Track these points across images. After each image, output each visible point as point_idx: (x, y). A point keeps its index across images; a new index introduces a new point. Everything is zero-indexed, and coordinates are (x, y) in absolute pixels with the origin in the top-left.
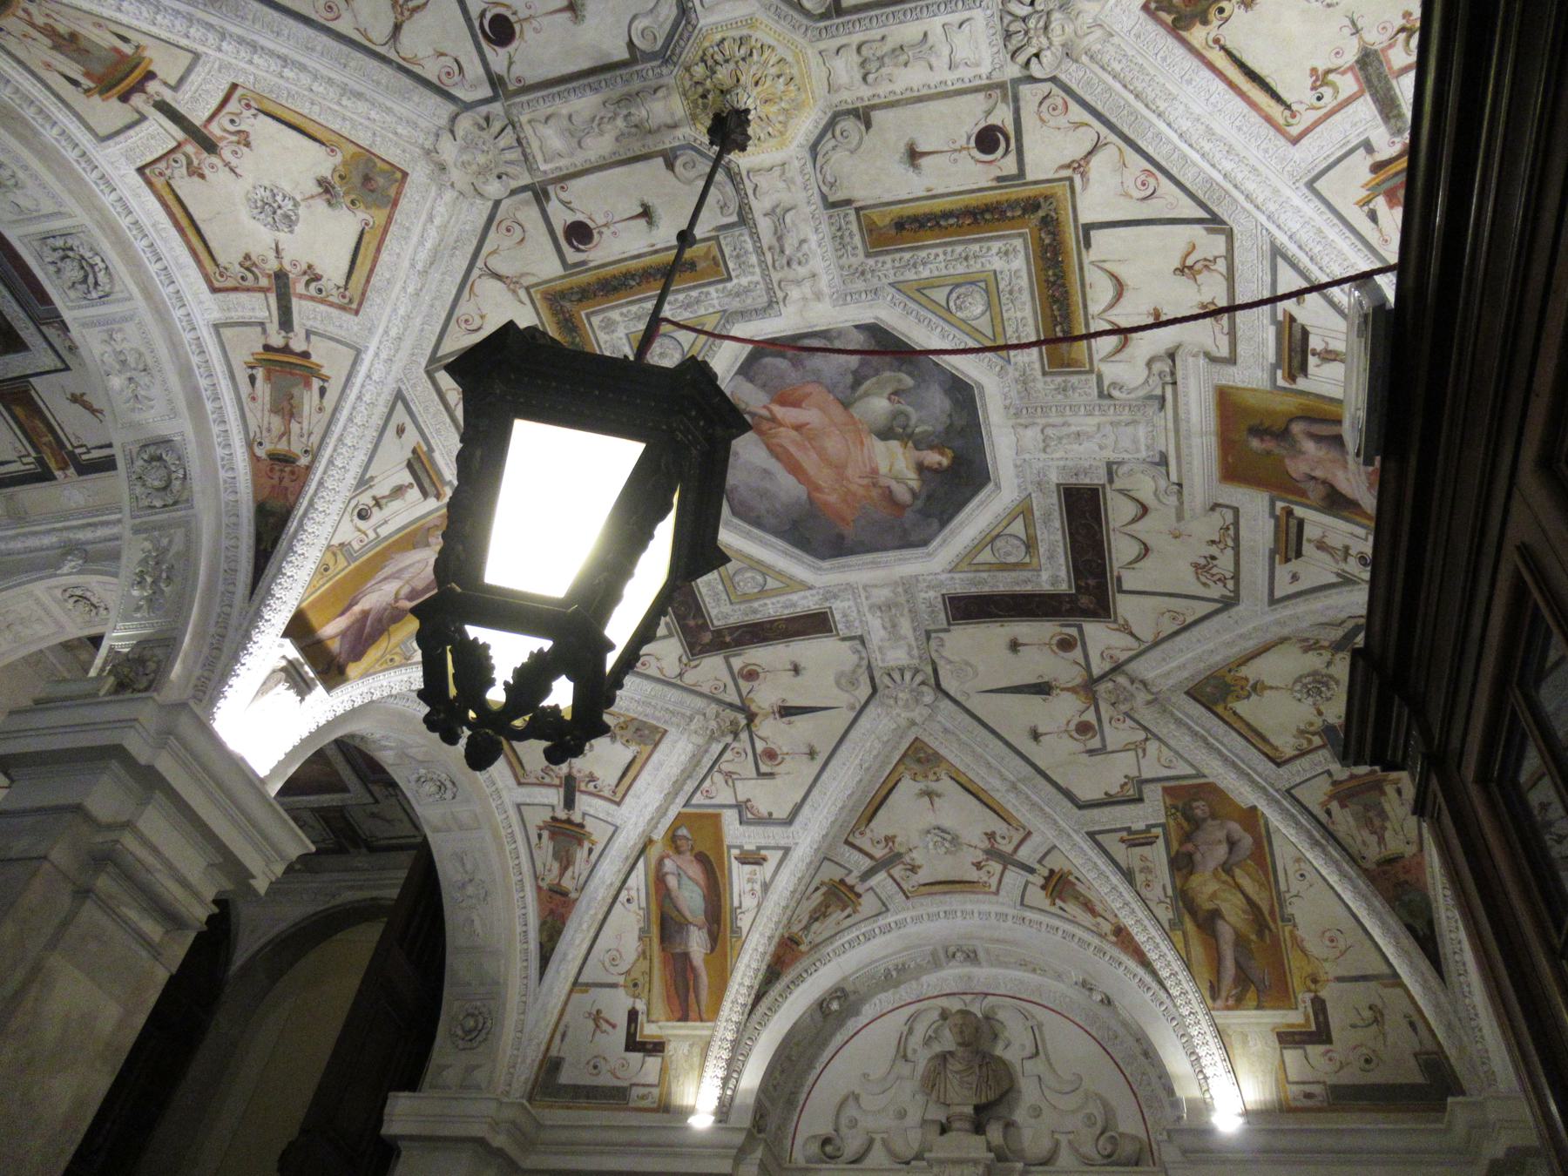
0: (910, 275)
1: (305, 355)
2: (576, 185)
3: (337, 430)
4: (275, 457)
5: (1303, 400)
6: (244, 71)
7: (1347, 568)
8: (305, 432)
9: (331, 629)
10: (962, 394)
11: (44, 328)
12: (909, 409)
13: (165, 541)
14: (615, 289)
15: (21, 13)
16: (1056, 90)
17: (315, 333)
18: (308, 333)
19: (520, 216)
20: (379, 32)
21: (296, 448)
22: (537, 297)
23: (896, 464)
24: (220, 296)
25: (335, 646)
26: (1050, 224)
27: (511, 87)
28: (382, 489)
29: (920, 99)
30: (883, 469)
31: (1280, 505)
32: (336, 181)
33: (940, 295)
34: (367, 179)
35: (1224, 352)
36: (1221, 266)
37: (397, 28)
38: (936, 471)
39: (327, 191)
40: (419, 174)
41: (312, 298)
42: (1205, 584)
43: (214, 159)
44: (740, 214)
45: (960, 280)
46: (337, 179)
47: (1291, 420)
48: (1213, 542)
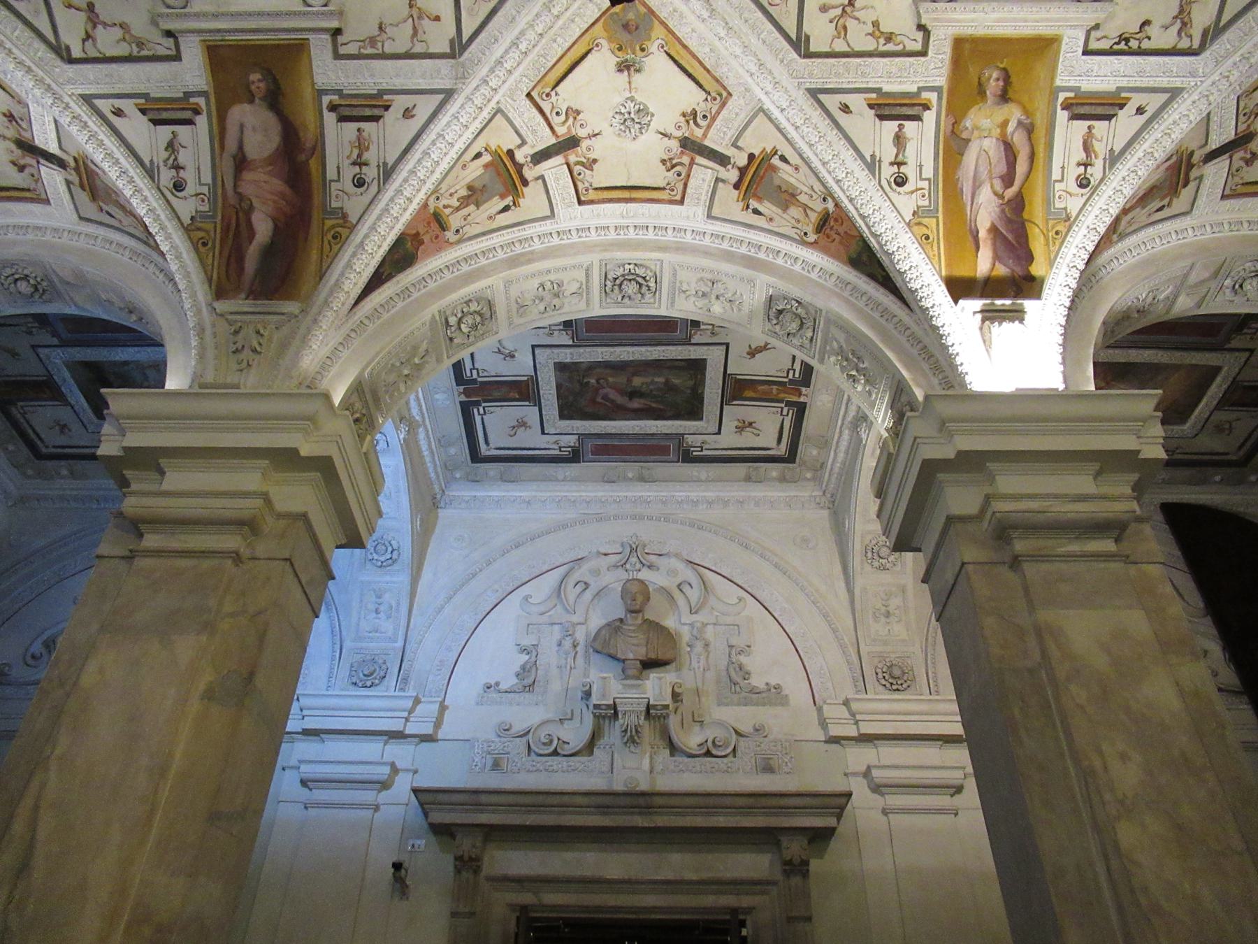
1: (751, 157)
3: (816, 163)
6: (518, 82)
8: (810, 192)
9: (984, 264)
11: (693, 341)
13: (835, 344)
15: (448, 211)
17: (737, 139)
18: (735, 145)
21: (818, 206)
25: (1002, 270)
28: (888, 153)
34: (626, 27)
39: (628, 68)
41: (709, 127)
43: (584, 144)
46: (619, 54)
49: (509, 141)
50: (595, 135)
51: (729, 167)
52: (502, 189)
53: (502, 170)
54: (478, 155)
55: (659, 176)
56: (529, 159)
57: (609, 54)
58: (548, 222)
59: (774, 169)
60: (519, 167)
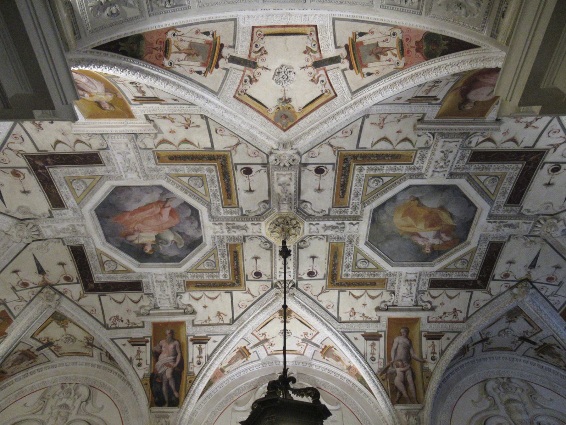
0: (219, 253)
1: (217, 66)
2: (265, 176)
4: (167, 44)
5: (185, 344)
7: (135, 360)
8: (181, 62)
10: (177, 259)
12: (169, 245)
14: (224, 175)
15: (395, 52)
16: (268, 289)
17: (227, 73)
18: (227, 70)
19: (258, 158)
20: (333, 142)
22: (226, 153)
23: (146, 237)
24: (250, 30)
26: (233, 285)
27: (302, 168)
29: (272, 262)
30: (142, 234)
31: (149, 339)
32: (288, 105)
33: (212, 258)
34: (286, 117)
35: (196, 323)
36: (221, 322)
37: (332, 146)
38: (143, 248)
39: (286, 100)
40: (285, 136)
41: (243, 77)
42: (110, 319)
43: (310, 63)
44: (245, 215)
45: (217, 263)
46: (289, 106)
47: (178, 341)
48: (129, 321)
49: (351, 74)
50: (303, 68)
51: (228, 57)
52: (361, 48)
53: (358, 59)
54: (369, 74)
55: (269, 43)
56: (342, 61)
57: (295, 106)
58: (337, 16)
59: (203, 65)
60: (348, 57)
